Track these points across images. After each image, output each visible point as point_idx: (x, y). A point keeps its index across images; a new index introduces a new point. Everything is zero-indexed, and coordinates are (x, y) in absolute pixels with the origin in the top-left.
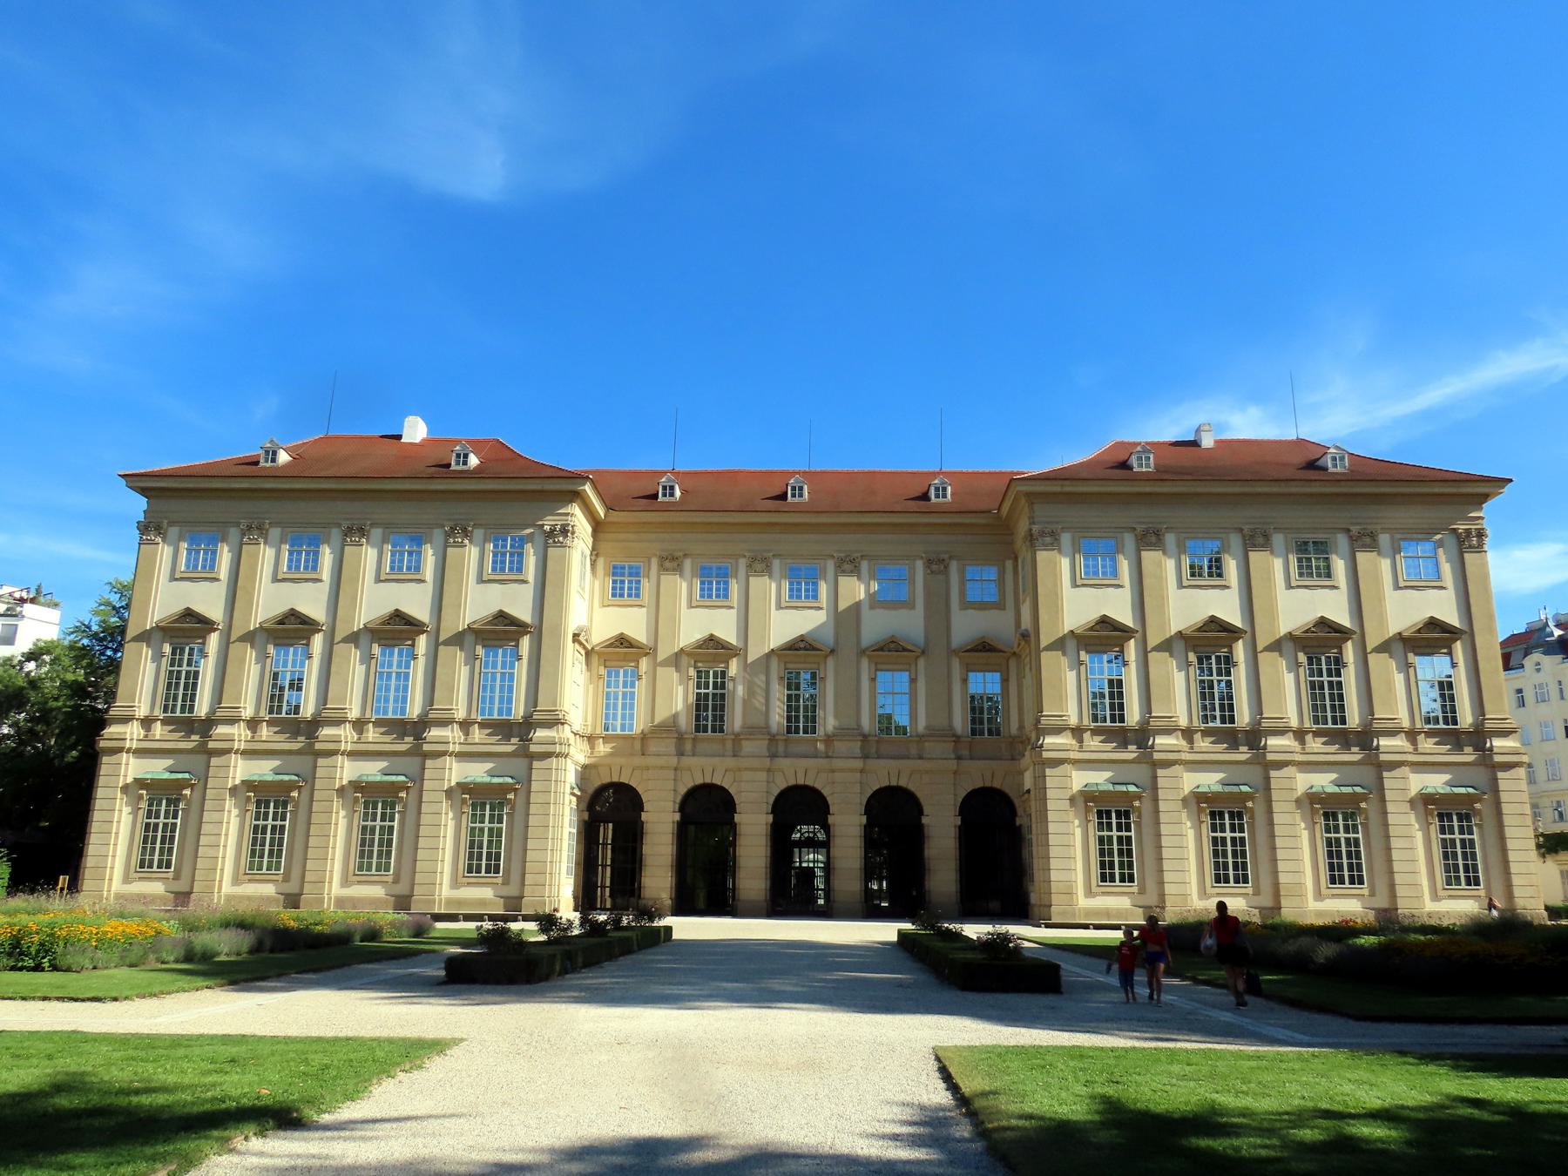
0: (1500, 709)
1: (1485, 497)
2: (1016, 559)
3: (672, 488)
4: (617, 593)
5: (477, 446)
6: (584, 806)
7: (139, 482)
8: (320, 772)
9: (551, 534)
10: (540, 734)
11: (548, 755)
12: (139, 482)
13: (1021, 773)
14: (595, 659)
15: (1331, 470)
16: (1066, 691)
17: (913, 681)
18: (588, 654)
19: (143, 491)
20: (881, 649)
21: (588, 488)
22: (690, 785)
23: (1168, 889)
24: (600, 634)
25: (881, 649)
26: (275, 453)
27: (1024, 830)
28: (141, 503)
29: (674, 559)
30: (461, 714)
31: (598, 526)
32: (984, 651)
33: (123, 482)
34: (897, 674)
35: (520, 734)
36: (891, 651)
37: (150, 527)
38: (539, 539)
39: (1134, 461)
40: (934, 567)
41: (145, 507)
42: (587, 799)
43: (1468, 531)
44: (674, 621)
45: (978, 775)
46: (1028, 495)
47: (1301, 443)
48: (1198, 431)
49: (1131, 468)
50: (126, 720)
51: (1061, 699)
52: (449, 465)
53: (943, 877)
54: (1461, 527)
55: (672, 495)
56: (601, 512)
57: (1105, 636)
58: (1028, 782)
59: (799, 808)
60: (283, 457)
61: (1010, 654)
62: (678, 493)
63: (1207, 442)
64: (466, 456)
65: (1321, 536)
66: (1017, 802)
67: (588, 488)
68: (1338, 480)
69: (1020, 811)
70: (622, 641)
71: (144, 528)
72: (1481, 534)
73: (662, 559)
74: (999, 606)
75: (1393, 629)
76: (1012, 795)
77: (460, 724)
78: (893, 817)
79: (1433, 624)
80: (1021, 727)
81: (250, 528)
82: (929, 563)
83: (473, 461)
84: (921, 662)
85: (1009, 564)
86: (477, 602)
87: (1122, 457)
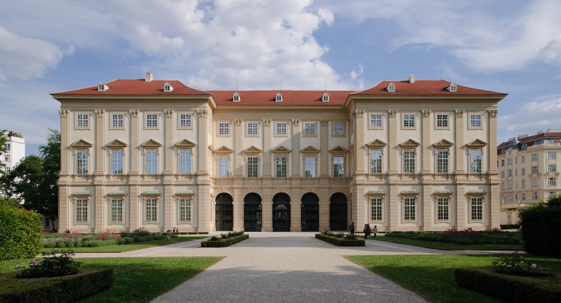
0: (494, 168)
1: (498, 100)
5: (172, 83)
13: (349, 188)
15: (451, 91)
21: (211, 98)
36: (310, 151)
39: (388, 89)
43: (492, 111)
45: (337, 188)
46: (355, 100)
49: (387, 91)
52: (163, 90)
56: (215, 105)
57: (378, 145)
58: (351, 191)
61: (347, 152)
64: (169, 87)
67: (211, 98)
68: (453, 94)
69: (348, 199)
72: (496, 112)
78: (310, 202)
80: (349, 174)
83: (171, 89)
87: (384, 87)
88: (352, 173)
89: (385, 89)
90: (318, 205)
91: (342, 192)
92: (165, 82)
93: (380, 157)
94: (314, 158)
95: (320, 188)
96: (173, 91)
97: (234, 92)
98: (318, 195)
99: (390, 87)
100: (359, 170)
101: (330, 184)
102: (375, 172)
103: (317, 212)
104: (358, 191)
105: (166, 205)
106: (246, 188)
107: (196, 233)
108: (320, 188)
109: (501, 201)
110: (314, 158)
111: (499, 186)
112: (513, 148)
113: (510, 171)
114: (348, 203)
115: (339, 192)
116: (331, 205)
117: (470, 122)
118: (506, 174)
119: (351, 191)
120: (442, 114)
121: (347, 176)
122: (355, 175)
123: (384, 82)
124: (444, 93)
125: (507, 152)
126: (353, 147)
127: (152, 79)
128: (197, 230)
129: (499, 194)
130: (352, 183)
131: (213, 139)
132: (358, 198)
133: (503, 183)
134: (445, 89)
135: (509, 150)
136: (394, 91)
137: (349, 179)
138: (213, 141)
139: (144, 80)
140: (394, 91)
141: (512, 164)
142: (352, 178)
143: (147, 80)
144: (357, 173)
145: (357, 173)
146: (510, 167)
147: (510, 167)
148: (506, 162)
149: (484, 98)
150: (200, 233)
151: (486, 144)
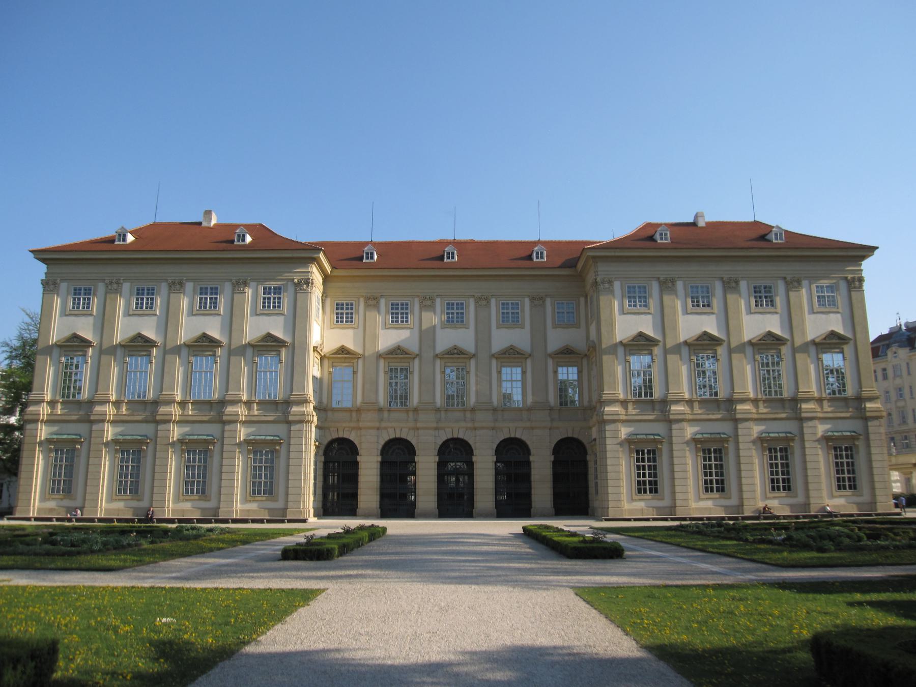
0: (871, 387)
1: (863, 258)
2: (586, 297)
3: (372, 254)
4: (339, 319)
5: (251, 228)
6: (321, 452)
7: (42, 255)
8: (160, 434)
9: (299, 284)
10: (295, 409)
11: (301, 422)
12: (42, 255)
13: (590, 428)
14: (326, 362)
15: (774, 241)
16: (618, 379)
17: (524, 373)
18: (322, 358)
19: (43, 260)
20: (505, 353)
21: (321, 256)
22: (387, 438)
23: (678, 496)
24: (329, 347)
25: (505, 353)
26: (125, 236)
28: (43, 268)
29: (375, 298)
30: (245, 398)
31: (326, 279)
32: (567, 355)
33: (32, 255)
34: (514, 369)
35: (281, 409)
36: (511, 355)
37: (49, 285)
38: (291, 289)
39: (657, 237)
40: (536, 302)
41: (45, 270)
42: (323, 447)
43: (853, 278)
44: (375, 337)
45: (565, 430)
46: (594, 257)
47: (756, 223)
48: (696, 216)
49: (655, 241)
50: (39, 402)
51: (614, 385)
52: (233, 242)
54: (850, 276)
55: (372, 258)
56: (328, 269)
57: (641, 343)
58: (594, 433)
59: (455, 453)
60: (130, 238)
61: (586, 356)
62: (376, 257)
63: (701, 224)
64: (244, 236)
65: (768, 283)
66: (588, 446)
67: (321, 256)
68: (779, 247)
69: (589, 451)
70: (343, 350)
71: (45, 283)
72: (861, 280)
73: (367, 299)
74: (577, 326)
75: (810, 337)
76: (585, 441)
77: (245, 403)
78: (512, 455)
79: (833, 334)
80: (590, 401)
81: (111, 283)
82: (533, 299)
83: (249, 239)
84: (529, 362)
85: (582, 300)
86: (253, 328)
88: (595, 398)
89: (651, 238)
90: (528, 463)
91: (575, 436)
92: (237, 226)
93: (649, 366)
94: (519, 370)
95: (533, 428)
96: (251, 243)
97: (366, 244)
98: (528, 442)
99: (661, 234)
100: (607, 393)
101: (552, 420)
102: (640, 396)
103: (527, 478)
104: (608, 434)
105: (225, 462)
106: (386, 428)
107: (282, 521)
108: (533, 428)
109: (889, 449)
110: (519, 370)
111: (882, 420)
112: (900, 346)
113: (900, 389)
114: (588, 458)
115: (570, 435)
116: (554, 463)
117: (815, 299)
118: (893, 395)
119: (594, 433)
120: (762, 283)
121: (586, 403)
122: (603, 403)
123: (649, 225)
124: (762, 244)
125: (890, 354)
126: (594, 348)
127: (214, 221)
128: (217, 514)
129: (884, 437)
130: (595, 418)
131: (321, 333)
132: (608, 448)
133: (890, 414)
134: (763, 238)
135: (894, 348)
136: (669, 241)
137: (592, 410)
138: (323, 337)
139: (200, 223)
140: (669, 241)
141: (901, 376)
142: (595, 408)
143: (204, 224)
144: (604, 397)
145: (604, 397)
146: (898, 381)
147: (898, 381)
148: (890, 372)
149: (835, 254)
150: (290, 521)
151: (850, 339)
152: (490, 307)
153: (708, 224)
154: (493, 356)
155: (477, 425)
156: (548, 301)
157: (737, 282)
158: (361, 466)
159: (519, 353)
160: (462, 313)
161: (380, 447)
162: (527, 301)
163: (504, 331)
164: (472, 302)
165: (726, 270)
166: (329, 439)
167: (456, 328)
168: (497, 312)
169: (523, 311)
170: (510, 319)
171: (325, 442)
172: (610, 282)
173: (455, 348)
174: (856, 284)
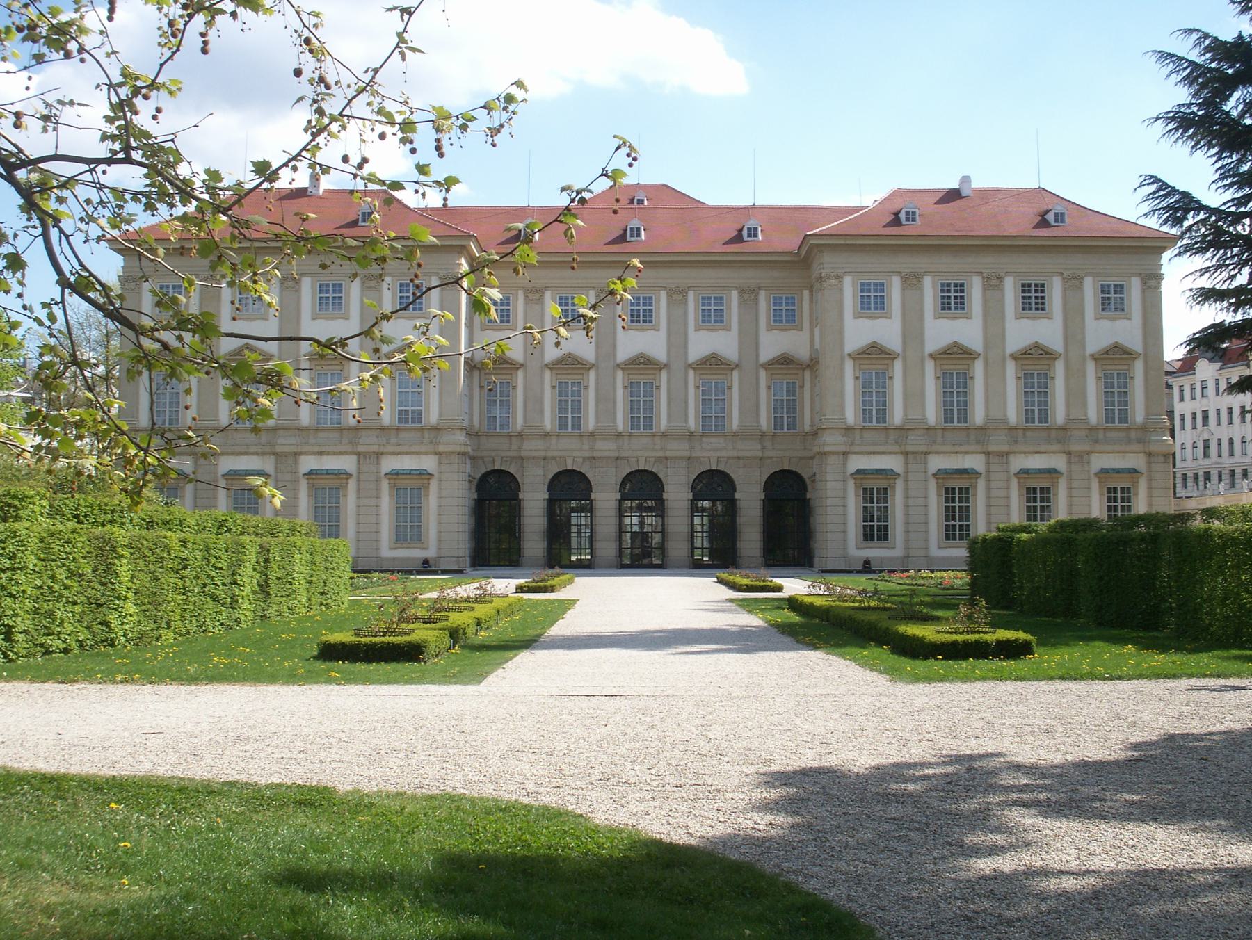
19: (119, 251)
20: (705, 363)
25: (705, 363)
27: (812, 502)
40: (746, 296)
42: (475, 482)
47: (1041, 191)
53: (751, 539)
66: (808, 481)
72: (1159, 278)
76: (805, 476)
82: (742, 292)
85: (806, 293)
95: (739, 458)
98: (733, 476)
101: (763, 448)
115: (786, 468)
152: (686, 303)
153: (975, 190)
154: (690, 365)
155: (668, 454)
156: (762, 294)
157: (1001, 279)
158: (525, 504)
159: (722, 363)
160: (651, 311)
161: (548, 481)
162: (735, 293)
163: (704, 334)
164: (663, 294)
165: (989, 262)
166: (483, 471)
167: (643, 330)
168: (696, 309)
169: (729, 308)
170: (713, 317)
171: (478, 476)
172: (839, 278)
173: (642, 355)
174: (1152, 281)
